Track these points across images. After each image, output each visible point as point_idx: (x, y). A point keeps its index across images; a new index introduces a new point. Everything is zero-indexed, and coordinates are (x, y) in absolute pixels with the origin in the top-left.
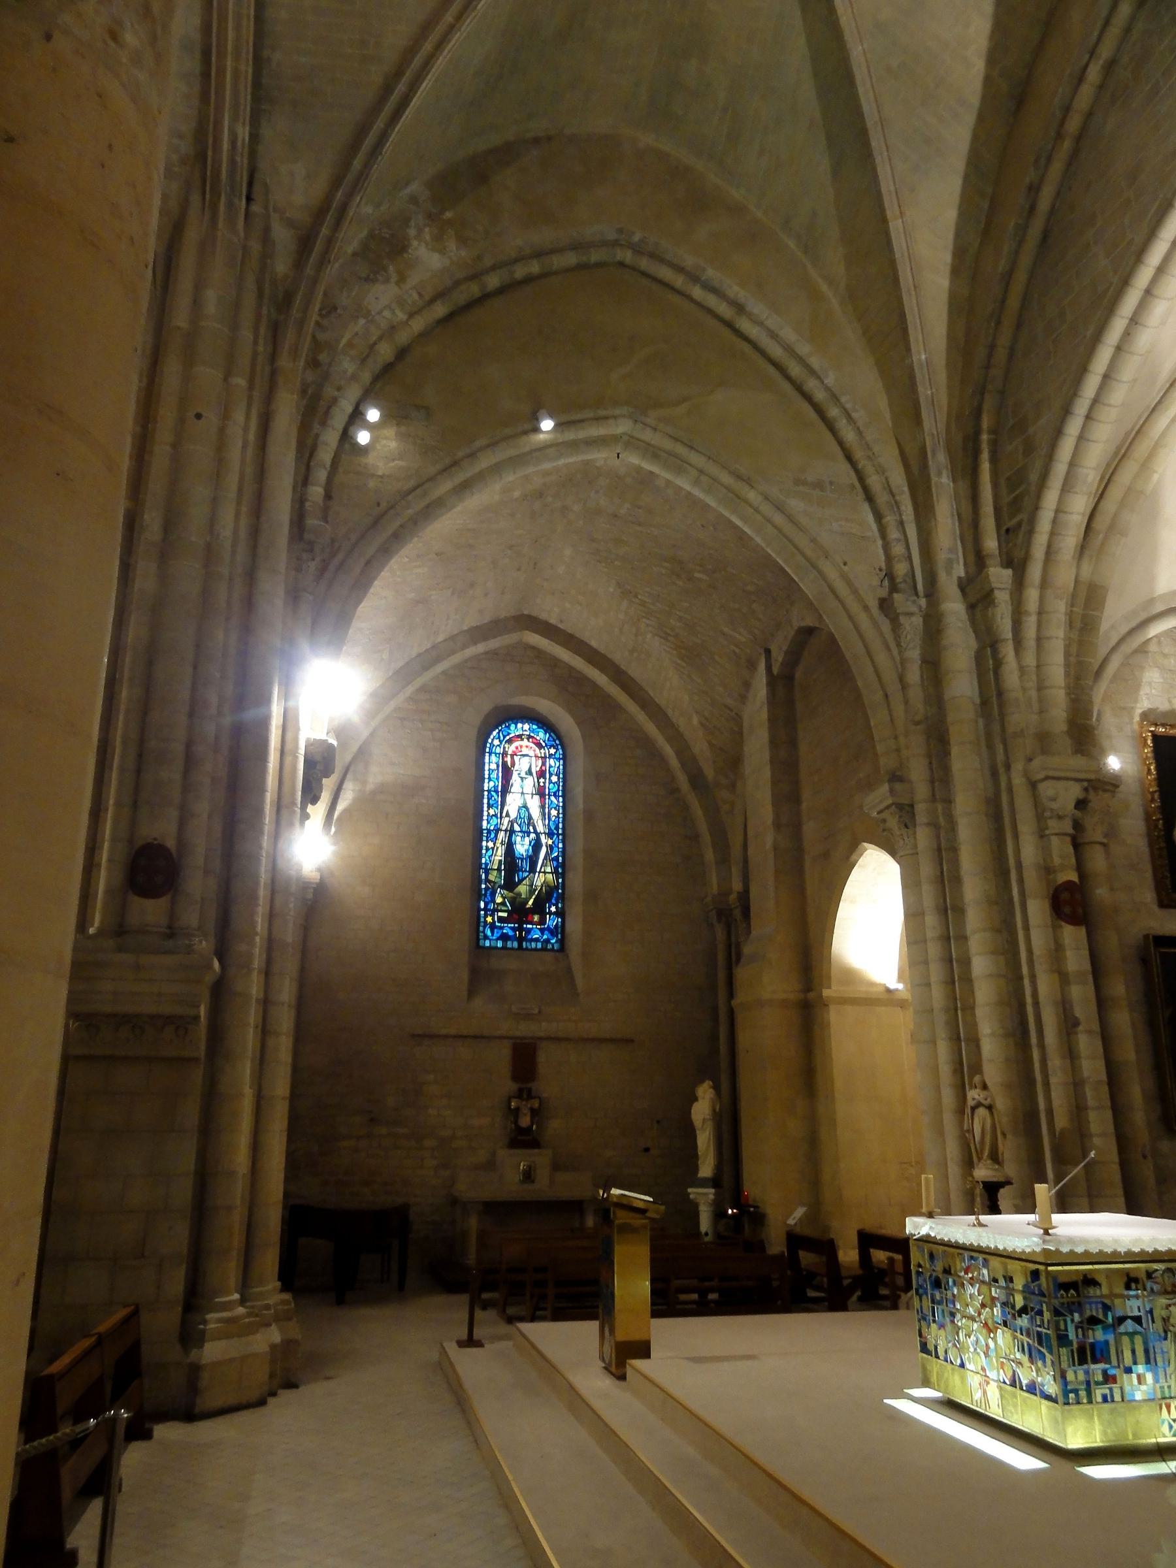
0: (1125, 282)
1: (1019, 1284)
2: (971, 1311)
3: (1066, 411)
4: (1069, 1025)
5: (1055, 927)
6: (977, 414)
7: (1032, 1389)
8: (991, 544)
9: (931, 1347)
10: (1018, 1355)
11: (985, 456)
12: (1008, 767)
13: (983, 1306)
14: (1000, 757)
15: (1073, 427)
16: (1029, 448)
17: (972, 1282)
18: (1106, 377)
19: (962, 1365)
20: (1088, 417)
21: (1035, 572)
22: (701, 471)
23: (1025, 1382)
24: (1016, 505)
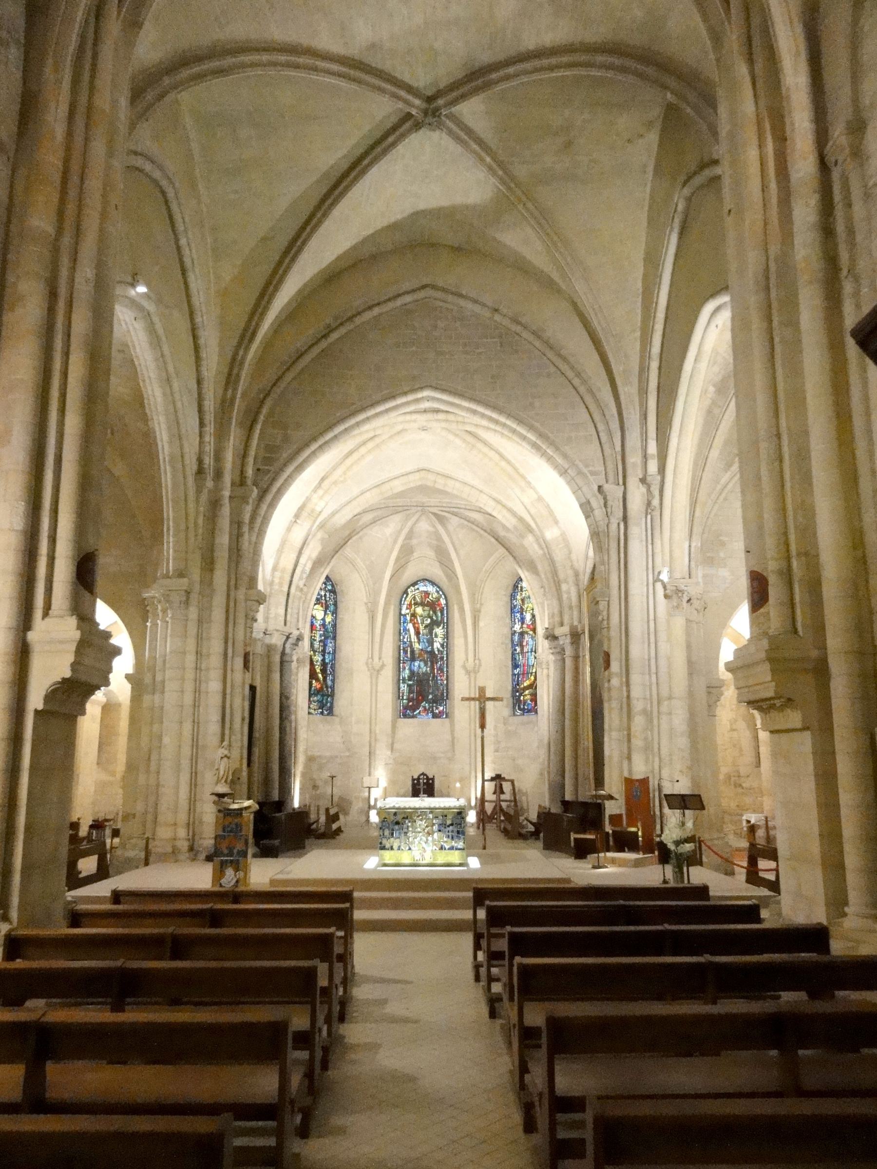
0: (363, 409)
1: (450, 817)
2: (419, 830)
3: (314, 439)
4: (243, 719)
5: (244, 673)
6: (262, 402)
7: (452, 848)
8: (250, 472)
9: (388, 846)
10: (445, 839)
11: (258, 427)
12: (236, 588)
13: (427, 827)
14: (233, 583)
15: (314, 446)
16: (286, 439)
17: (421, 820)
18: (336, 436)
19: (410, 849)
20: (320, 447)
21: (269, 498)
22: (163, 356)
23: (447, 847)
24: (268, 461)
